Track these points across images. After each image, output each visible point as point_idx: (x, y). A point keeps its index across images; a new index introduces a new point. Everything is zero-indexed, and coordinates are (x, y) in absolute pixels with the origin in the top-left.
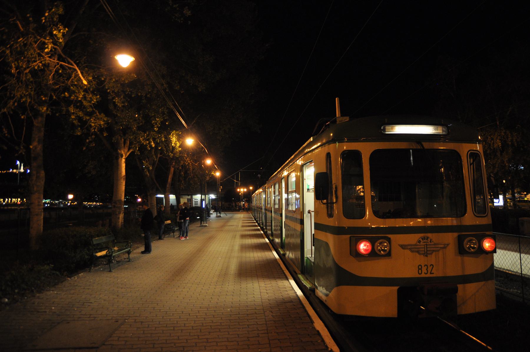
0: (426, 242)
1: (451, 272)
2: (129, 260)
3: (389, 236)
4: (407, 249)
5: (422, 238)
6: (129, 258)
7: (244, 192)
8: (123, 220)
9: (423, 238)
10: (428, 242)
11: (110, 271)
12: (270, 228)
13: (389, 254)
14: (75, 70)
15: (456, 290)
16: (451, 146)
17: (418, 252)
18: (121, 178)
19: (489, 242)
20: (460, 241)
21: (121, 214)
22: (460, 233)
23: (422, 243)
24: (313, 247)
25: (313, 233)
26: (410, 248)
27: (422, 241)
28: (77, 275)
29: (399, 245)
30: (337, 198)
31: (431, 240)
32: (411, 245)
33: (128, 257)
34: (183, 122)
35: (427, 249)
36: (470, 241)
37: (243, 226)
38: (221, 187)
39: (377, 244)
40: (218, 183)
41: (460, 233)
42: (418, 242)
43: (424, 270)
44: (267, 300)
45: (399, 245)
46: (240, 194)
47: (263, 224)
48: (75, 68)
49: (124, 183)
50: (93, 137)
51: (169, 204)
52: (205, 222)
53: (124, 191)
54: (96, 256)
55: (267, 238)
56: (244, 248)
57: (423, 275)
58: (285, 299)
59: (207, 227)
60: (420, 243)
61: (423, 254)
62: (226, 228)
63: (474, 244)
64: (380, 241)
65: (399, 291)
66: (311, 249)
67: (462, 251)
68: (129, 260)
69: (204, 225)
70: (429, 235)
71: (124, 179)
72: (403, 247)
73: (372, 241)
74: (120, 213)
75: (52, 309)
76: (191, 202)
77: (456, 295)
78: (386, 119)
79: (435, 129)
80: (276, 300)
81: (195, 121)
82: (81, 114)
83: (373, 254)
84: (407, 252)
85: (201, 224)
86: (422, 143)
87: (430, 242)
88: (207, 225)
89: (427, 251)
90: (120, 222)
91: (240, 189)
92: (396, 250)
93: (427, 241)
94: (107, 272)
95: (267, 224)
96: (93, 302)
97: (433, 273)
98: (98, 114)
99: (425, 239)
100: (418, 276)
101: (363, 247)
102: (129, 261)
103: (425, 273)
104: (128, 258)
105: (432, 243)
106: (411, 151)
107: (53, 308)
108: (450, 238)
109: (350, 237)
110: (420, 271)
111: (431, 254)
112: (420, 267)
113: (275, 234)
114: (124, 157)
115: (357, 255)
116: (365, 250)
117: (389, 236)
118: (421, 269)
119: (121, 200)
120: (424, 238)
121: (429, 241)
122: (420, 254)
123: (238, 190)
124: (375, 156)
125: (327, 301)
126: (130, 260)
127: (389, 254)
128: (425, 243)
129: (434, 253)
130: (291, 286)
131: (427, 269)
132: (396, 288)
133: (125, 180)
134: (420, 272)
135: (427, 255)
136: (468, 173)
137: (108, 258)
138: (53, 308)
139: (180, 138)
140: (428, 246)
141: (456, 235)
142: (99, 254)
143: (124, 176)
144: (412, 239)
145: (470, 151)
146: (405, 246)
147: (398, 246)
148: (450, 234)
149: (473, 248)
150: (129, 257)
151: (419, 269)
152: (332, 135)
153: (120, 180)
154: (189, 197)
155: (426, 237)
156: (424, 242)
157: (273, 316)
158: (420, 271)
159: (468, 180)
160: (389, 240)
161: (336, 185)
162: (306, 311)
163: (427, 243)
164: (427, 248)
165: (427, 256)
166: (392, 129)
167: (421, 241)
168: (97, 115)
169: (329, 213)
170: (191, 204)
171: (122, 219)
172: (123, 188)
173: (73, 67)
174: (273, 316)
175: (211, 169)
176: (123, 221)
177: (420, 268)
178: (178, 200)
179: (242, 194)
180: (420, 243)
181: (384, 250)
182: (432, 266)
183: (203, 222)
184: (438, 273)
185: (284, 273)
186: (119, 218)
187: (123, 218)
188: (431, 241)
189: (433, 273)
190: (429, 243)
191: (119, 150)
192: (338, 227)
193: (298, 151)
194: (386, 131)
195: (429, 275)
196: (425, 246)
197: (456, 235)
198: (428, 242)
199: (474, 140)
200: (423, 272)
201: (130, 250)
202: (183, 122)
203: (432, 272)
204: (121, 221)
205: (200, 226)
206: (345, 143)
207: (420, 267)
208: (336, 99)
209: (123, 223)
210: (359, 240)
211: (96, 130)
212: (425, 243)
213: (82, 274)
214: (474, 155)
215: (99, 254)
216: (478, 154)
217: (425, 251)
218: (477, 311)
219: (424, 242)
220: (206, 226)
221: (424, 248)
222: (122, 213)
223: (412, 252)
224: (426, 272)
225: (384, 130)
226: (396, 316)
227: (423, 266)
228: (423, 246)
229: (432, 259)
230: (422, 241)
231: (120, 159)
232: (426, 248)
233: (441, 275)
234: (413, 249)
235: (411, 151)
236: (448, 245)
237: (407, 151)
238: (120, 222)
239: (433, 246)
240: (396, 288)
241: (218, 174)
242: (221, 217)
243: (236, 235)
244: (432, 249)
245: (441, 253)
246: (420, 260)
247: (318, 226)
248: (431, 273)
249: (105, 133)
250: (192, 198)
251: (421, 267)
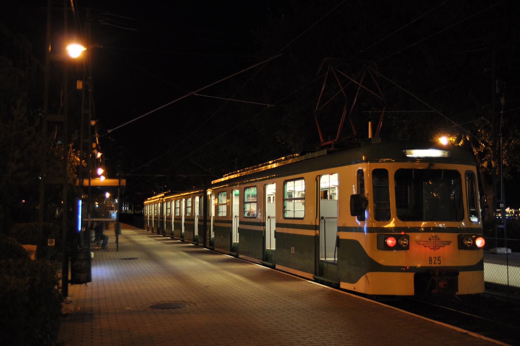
3: (408, 234)
5: (432, 237)
10: (436, 240)
15: (458, 274)
22: (459, 234)
23: (432, 241)
31: (438, 238)
35: (435, 245)
41: (459, 234)
42: (429, 239)
57: (433, 265)
60: (430, 240)
72: (418, 242)
77: (458, 277)
87: (438, 239)
89: (435, 246)
100: (429, 265)
101: (390, 242)
105: (440, 241)
108: (453, 237)
110: (430, 261)
112: (430, 259)
118: (431, 260)
121: (437, 239)
125: (355, 288)
128: (434, 241)
129: (441, 248)
145: (467, 171)
146: (420, 241)
151: (430, 260)
158: (430, 261)
159: (465, 194)
160: (408, 237)
163: (436, 241)
164: (435, 244)
167: (431, 239)
177: (430, 260)
180: (430, 240)
188: (439, 239)
190: (437, 240)
195: (437, 265)
196: (434, 242)
198: (436, 240)
207: (430, 259)
214: (470, 175)
216: (472, 173)
217: (434, 246)
219: (434, 240)
227: (433, 258)
228: (433, 243)
230: (432, 239)
232: (435, 244)
239: (440, 243)
251: (432, 259)
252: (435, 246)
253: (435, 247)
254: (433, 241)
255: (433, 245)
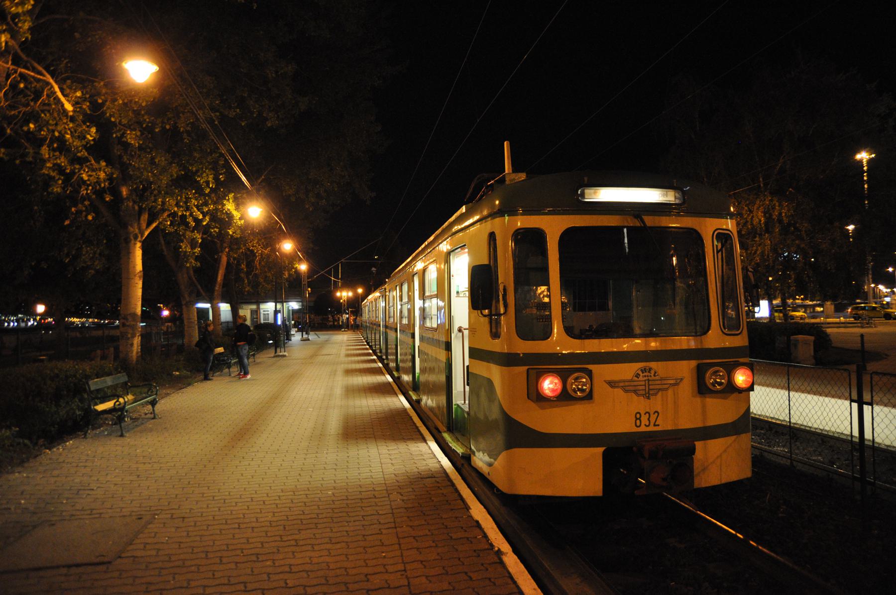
0: (648, 376)
1: (685, 424)
2: (154, 416)
3: (590, 367)
4: (617, 387)
5: (642, 370)
6: (154, 413)
7: (348, 298)
8: (140, 347)
9: (644, 370)
10: (650, 376)
11: (122, 435)
12: (394, 357)
13: (589, 397)
14: (48, 84)
15: (692, 451)
16: (688, 222)
17: (635, 392)
18: (135, 276)
19: (744, 374)
20: (700, 372)
21: (137, 338)
22: (700, 362)
23: (641, 378)
24: (467, 388)
25: (467, 363)
26: (622, 387)
27: (641, 374)
28: (63, 444)
29: (605, 381)
30: (506, 306)
31: (655, 373)
32: (624, 381)
33: (151, 411)
34: (243, 178)
36: (715, 373)
37: (348, 355)
38: (309, 289)
39: (571, 380)
40: (303, 283)
41: (700, 362)
42: (636, 376)
43: (644, 419)
44: (393, 475)
45: (605, 381)
46: (341, 301)
47: (381, 352)
48: (48, 80)
49: (140, 284)
50: (87, 203)
51: (219, 319)
52: (283, 350)
53: (141, 297)
54: (96, 410)
55: (389, 374)
56: (351, 391)
57: (643, 429)
58: (423, 473)
59: (285, 358)
60: (638, 378)
61: (643, 395)
62: (320, 358)
63: (722, 377)
64: (576, 375)
65: (605, 454)
66: (463, 390)
67: (702, 389)
68: (154, 416)
69: (281, 354)
70: (653, 365)
71: (140, 277)
72: (612, 384)
73: (564, 376)
74: (133, 336)
75: (20, 504)
76: (257, 315)
77: (693, 458)
78: (586, 179)
79: (663, 195)
80: (408, 474)
81: (263, 177)
82: (62, 161)
83: (565, 397)
84: (618, 392)
85: (276, 352)
86: (643, 217)
87: (654, 376)
88: (285, 353)
89: (649, 389)
90: (134, 353)
91: (341, 292)
92: (600, 389)
93: (649, 374)
94: (116, 436)
95: (389, 351)
96: (95, 488)
97: (658, 425)
98: (93, 162)
99: (646, 372)
100: (635, 430)
101: (549, 385)
102: (154, 418)
103: (645, 425)
104: (151, 413)
105: (657, 378)
106: (625, 230)
107: (23, 502)
108: (685, 369)
109: (528, 369)
110: (638, 422)
111: (656, 394)
112: (638, 416)
113: (402, 367)
114: (139, 239)
115: (539, 398)
116: (553, 390)
117: (590, 367)
118: (640, 419)
119: (135, 314)
120: (645, 369)
121: (652, 375)
122: (638, 395)
123: (338, 294)
124: (568, 237)
126: (157, 417)
127: (589, 397)
128: (647, 378)
129: (660, 393)
130: (432, 451)
131: (649, 419)
132: (602, 449)
133: (142, 279)
134: (638, 424)
135: (649, 396)
136: (713, 263)
137: (118, 414)
138: (23, 502)
139: (238, 204)
140: (650, 383)
141: (693, 363)
142: (101, 407)
143: (140, 272)
144: (626, 371)
146: (615, 382)
147: (604, 383)
148: (685, 363)
149: (720, 384)
150: (153, 410)
151: (637, 419)
152: (497, 202)
153: (133, 279)
154: (254, 307)
155: (648, 368)
156: (645, 376)
157: (403, 500)
158: (638, 422)
159: (713, 275)
160: (590, 374)
161: (504, 286)
162: (457, 491)
163: (649, 378)
164: (649, 385)
165: (648, 398)
166: (595, 193)
167: (640, 375)
168: (91, 164)
169: (494, 330)
170: (257, 318)
171: (138, 346)
172: (139, 292)
173: (45, 78)
174: (403, 500)
175: (293, 258)
176: (139, 350)
178: (235, 311)
179: (344, 301)
180: (638, 378)
181: (582, 390)
182: (656, 414)
183: (278, 350)
184: (665, 424)
185: (419, 431)
186: (132, 345)
187: (139, 344)
189: (658, 425)
191: (129, 227)
192: (509, 354)
193: (441, 228)
194: (586, 197)
195: (652, 428)
196: (647, 381)
197: (693, 363)
199: (722, 213)
200: (643, 424)
201: (155, 399)
202: (243, 178)
203: (656, 424)
204: (137, 350)
205: (274, 357)
206: (519, 217)
207: (638, 416)
208: (505, 143)
209: (140, 354)
210: (541, 374)
211: (89, 192)
212: (647, 378)
213: (71, 442)
214: (723, 237)
215: (101, 407)
216: (728, 234)
218: (723, 482)
219: (645, 376)
220: (284, 356)
221: (645, 385)
222: (138, 336)
223: (626, 391)
224: (647, 424)
225: (583, 195)
226: (600, 494)
227: (642, 413)
228: (643, 383)
229: (656, 403)
230: (641, 374)
231: (133, 242)
232: (647, 386)
233: (670, 428)
234: (628, 387)
235: (625, 230)
236: (682, 379)
237: (619, 229)
238: (134, 353)
239: (659, 382)
240: (601, 450)
241: (303, 267)
242: (309, 340)
243: (336, 371)
244: (658, 387)
245: (670, 392)
246: (639, 404)
247: (475, 353)
248: (655, 425)
249: (107, 196)
250: (258, 308)
252: (647, 389)
253: (647, 392)
254: (645, 378)
255: (643, 387)
